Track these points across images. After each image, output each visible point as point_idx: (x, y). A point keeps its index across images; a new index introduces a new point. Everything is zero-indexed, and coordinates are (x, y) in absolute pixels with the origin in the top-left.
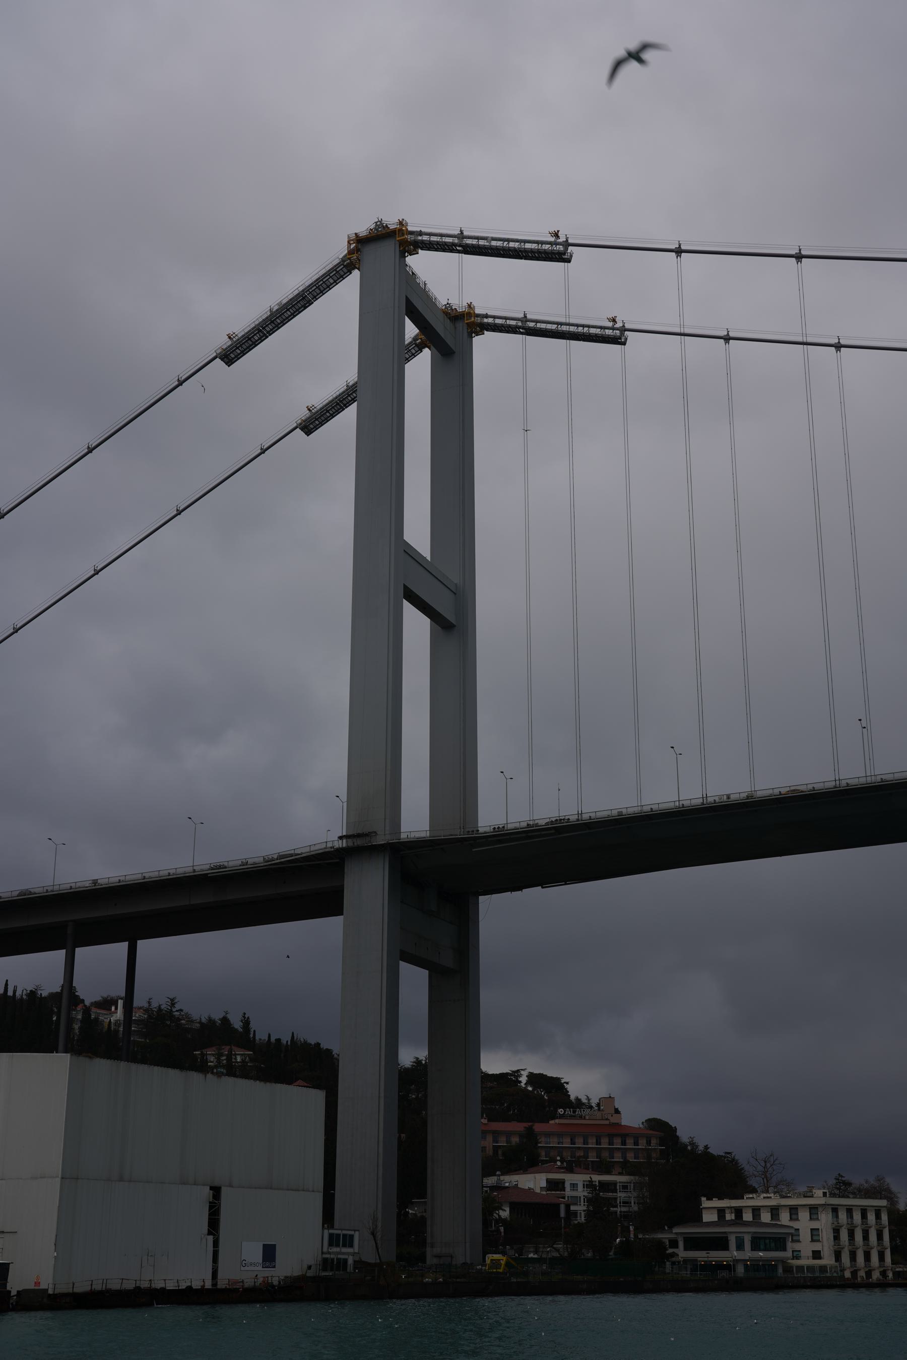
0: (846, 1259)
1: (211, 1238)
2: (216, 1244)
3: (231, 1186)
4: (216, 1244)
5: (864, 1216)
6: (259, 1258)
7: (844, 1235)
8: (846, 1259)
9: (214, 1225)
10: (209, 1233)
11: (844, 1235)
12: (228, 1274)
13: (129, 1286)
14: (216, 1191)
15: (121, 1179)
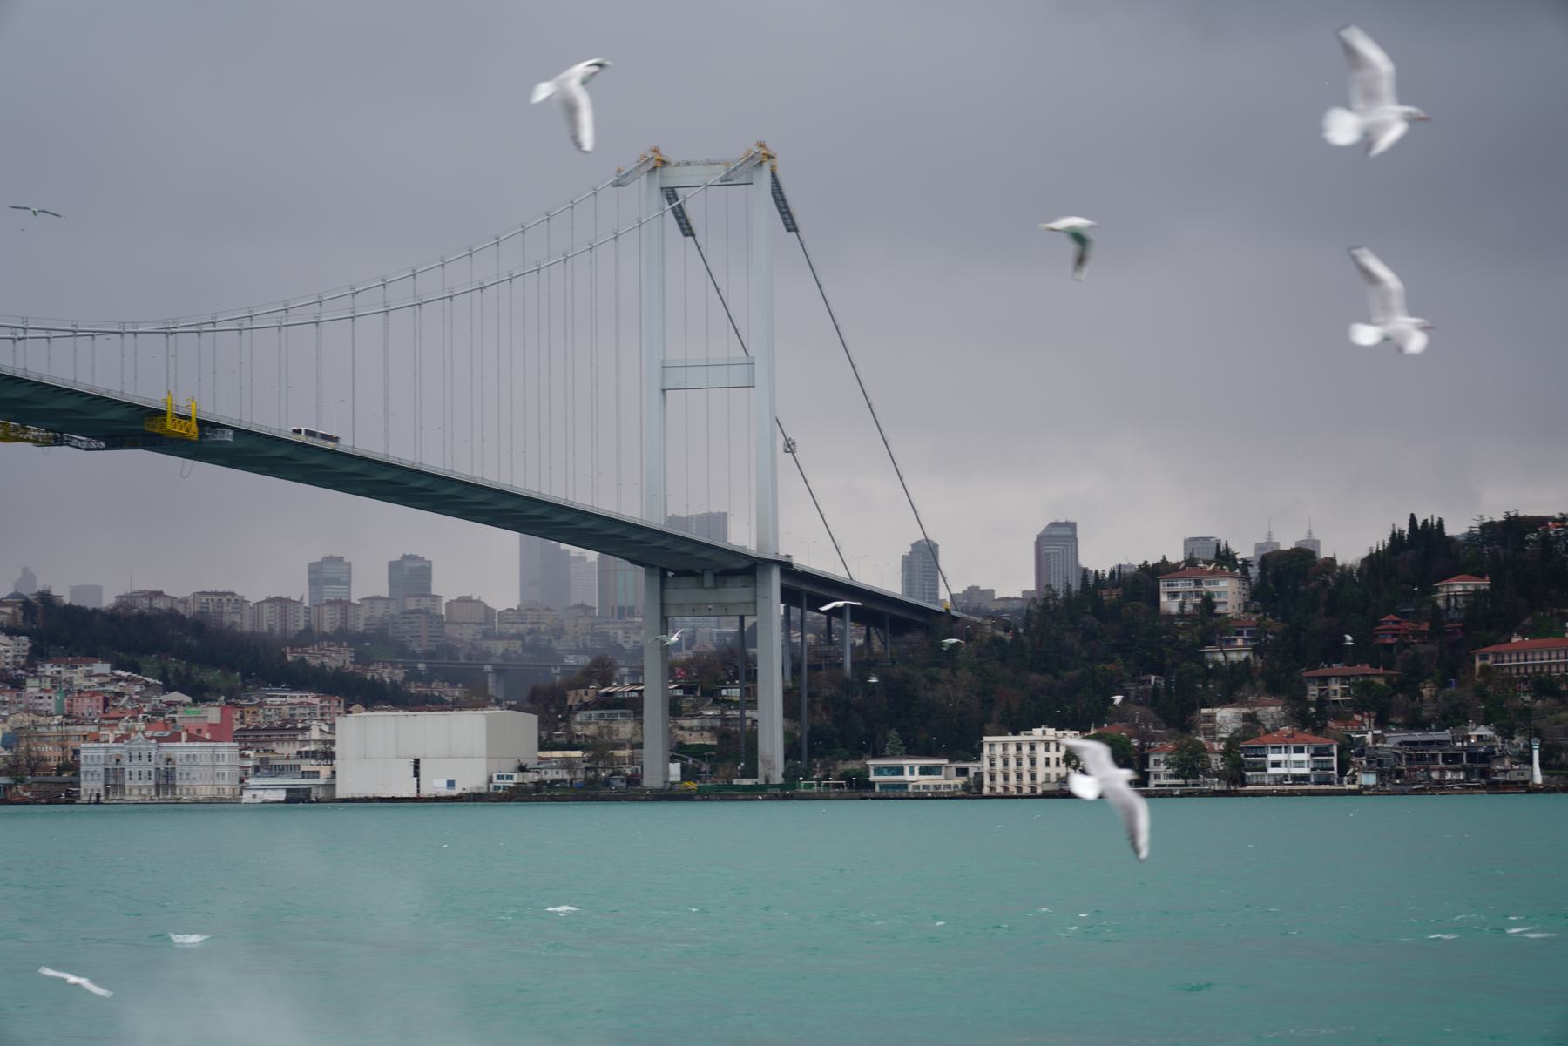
0: (1013, 779)
1: (416, 778)
2: (418, 780)
3: (426, 758)
4: (418, 780)
5: (1019, 747)
6: (445, 785)
7: (1012, 764)
8: (1013, 779)
9: (416, 774)
10: (415, 776)
11: (1012, 764)
12: (426, 791)
13: (390, 796)
14: (417, 762)
15: (365, 759)
